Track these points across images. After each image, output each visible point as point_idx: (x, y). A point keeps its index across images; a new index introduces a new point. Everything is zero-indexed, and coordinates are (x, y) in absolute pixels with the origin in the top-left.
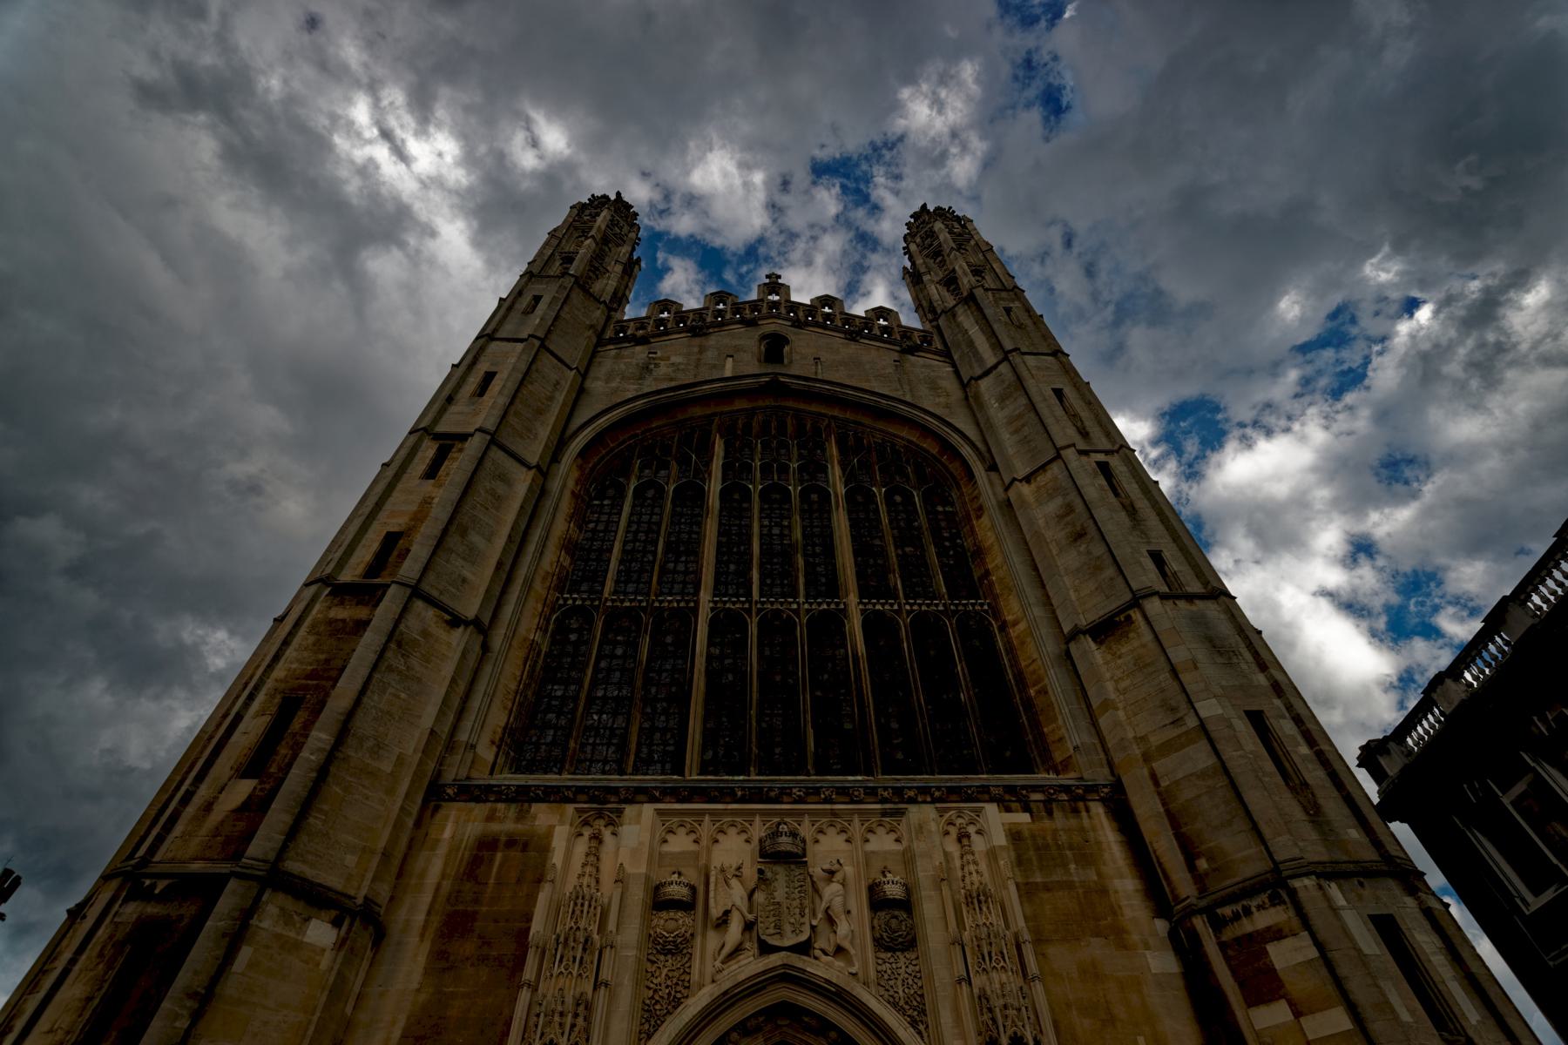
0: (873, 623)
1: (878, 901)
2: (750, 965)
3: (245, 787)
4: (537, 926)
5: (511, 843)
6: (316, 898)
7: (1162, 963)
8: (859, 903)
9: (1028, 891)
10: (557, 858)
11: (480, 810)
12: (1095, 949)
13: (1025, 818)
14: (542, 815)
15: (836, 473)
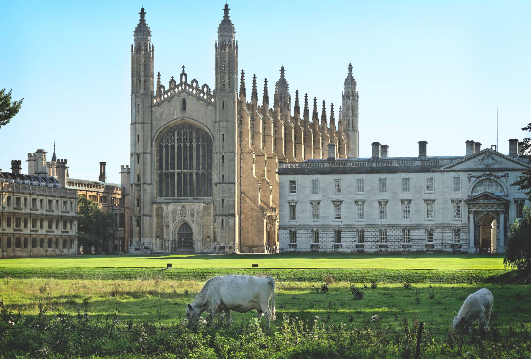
0: (197, 174)
1: (191, 213)
2: (180, 218)
3: (138, 208)
4: (164, 215)
5: (160, 208)
6: (147, 216)
7: (212, 218)
8: (190, 212)
9: (203, 212)
10: (164, 209)
11: (157, 204)
12: (208, 217)
13: (205, 205)
14: (162, 205)
15: (194, 141)
